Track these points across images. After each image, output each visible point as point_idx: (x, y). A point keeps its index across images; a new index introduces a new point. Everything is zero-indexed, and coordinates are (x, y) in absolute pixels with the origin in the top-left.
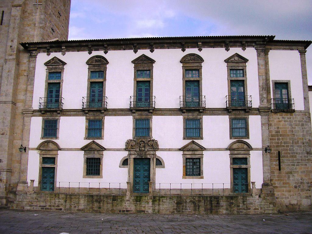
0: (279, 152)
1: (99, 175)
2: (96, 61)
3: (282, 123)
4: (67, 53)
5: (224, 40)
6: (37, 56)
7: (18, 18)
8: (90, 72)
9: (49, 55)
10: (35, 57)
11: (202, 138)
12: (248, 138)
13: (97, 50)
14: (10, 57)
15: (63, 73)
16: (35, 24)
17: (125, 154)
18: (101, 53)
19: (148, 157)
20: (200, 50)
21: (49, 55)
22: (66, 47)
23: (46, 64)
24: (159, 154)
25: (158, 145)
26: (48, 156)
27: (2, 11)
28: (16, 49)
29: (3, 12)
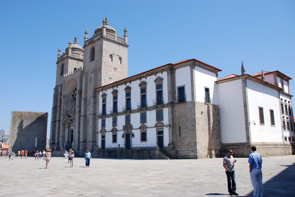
0: (180, 126)
1: (116, 142)
3: (181, 109)
4: (107, 90)
5: (153, 71)
9: (102, 92)
10: (99, 94)
11: (146, 123)
12: (163, 120)
13: (115, 87)
17: (123, 132)
19: (129, 133)
20: (146, 78)
22: (106, 88)
24: (133, 131)
25: (132, 127)
26: (103, 135)
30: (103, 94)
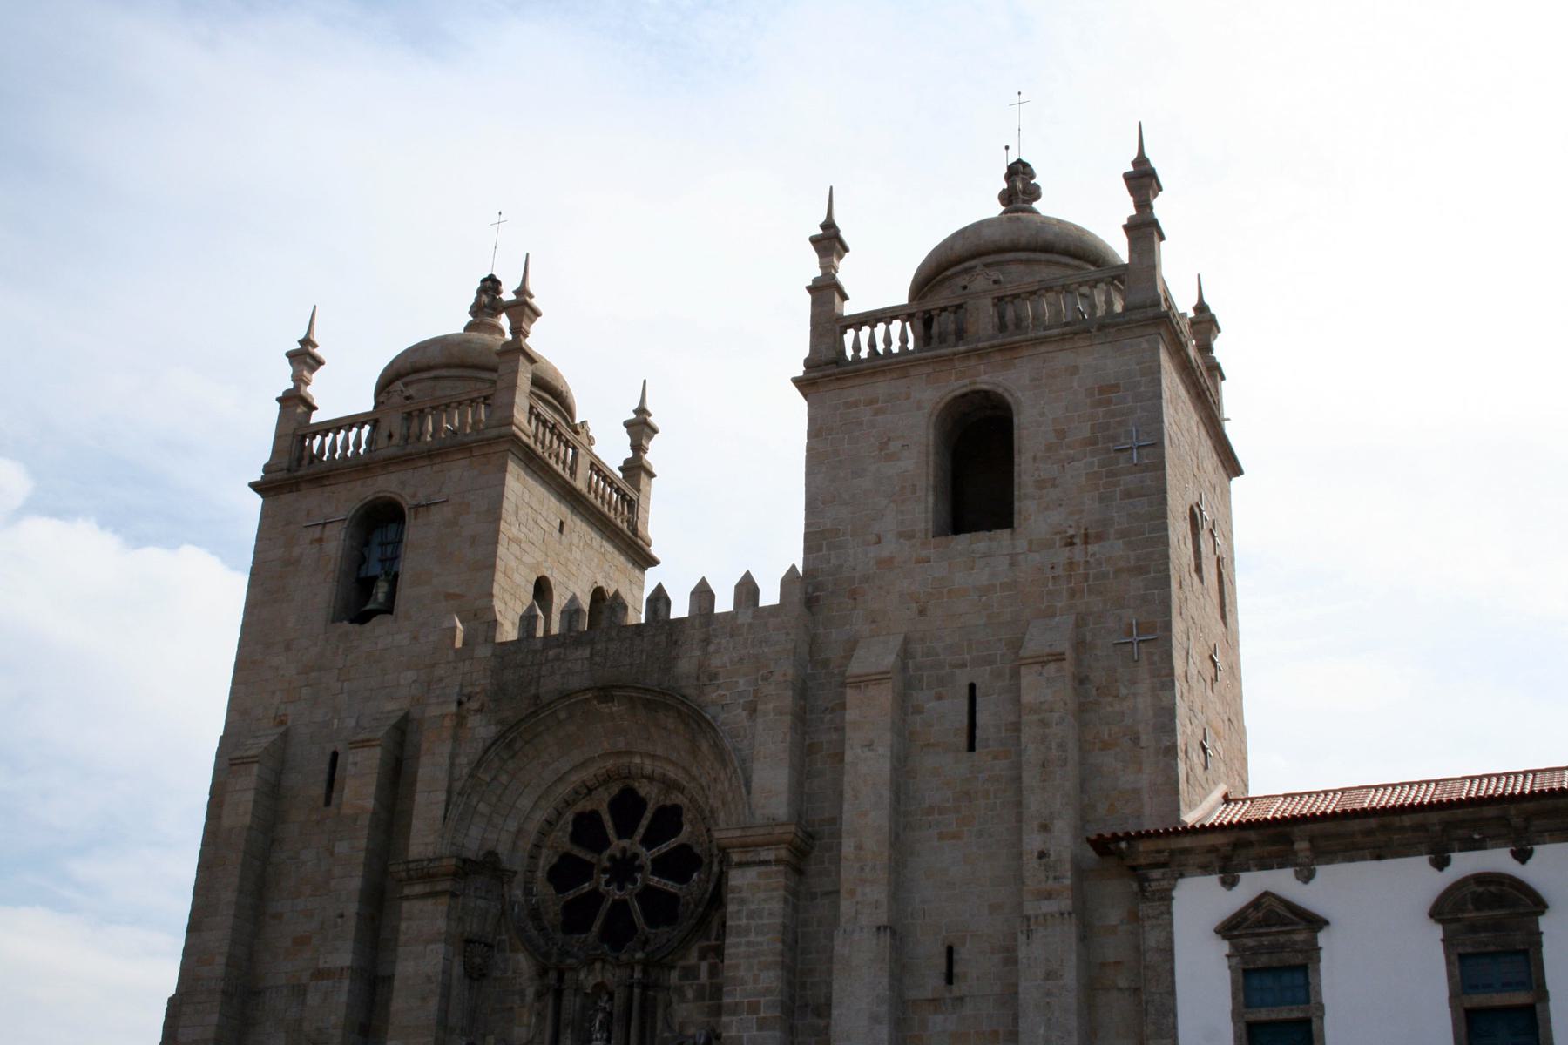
2: (1480, 902)
4: (1323, 872)
6: (1175, 893)
7: (1056, 716)
8: (1454, 958)
9: (1230, 882)
10: (1166, 898)
14: (1048, 907)
15: (1318, 971)
16: (1136, 740)
18: (1497, 860)
21: (1230, 882)
22: (1311, 841)
23: (1228, 930)
27: (966, 683)
28: (1068, 866)
29: (972, 687)
30: (1256, 904)
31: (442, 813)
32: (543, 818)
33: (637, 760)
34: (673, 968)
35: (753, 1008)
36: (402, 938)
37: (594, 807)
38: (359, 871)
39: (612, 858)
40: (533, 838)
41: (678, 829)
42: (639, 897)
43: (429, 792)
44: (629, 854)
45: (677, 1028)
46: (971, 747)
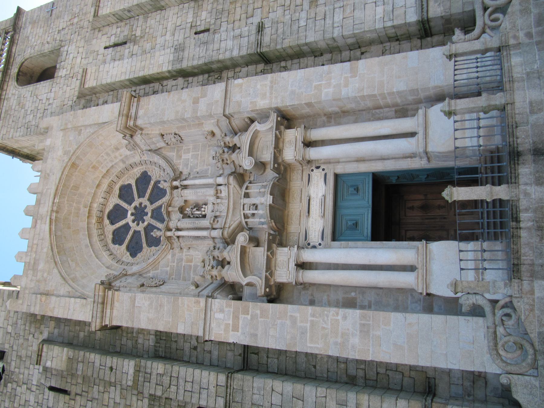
31: (78, 300)
32: (107, 257)
33: (95, 205)
34: (181, 173)
35: (196, 101)
36: (129, 325)
37: (111, 233)
38: (92, 356)
39: (133, 221)
40: (114, 263)
41: (130, 186)
42: (152, 203)
43: (69, 309)
44: (134, 211)
45: (209, 167)
46: (125, 43)
